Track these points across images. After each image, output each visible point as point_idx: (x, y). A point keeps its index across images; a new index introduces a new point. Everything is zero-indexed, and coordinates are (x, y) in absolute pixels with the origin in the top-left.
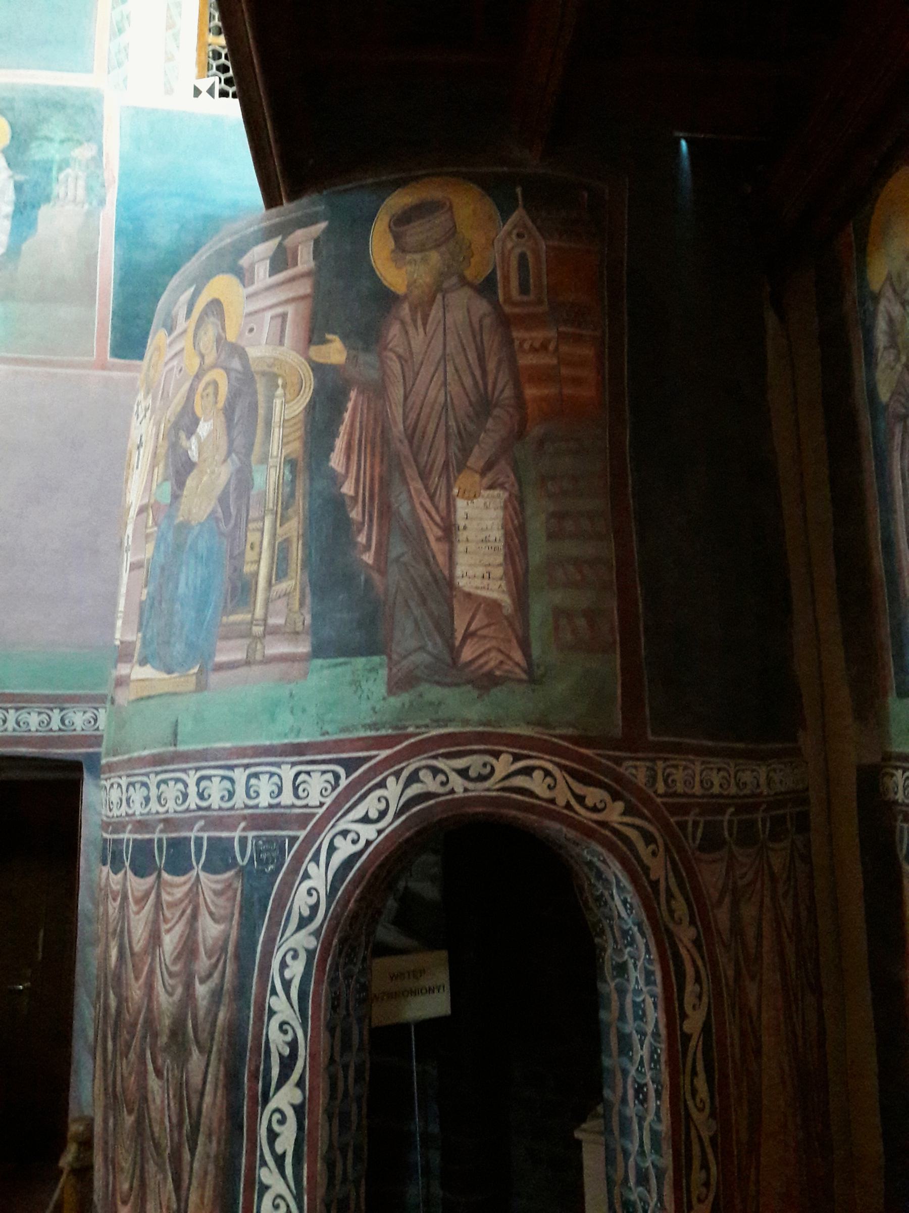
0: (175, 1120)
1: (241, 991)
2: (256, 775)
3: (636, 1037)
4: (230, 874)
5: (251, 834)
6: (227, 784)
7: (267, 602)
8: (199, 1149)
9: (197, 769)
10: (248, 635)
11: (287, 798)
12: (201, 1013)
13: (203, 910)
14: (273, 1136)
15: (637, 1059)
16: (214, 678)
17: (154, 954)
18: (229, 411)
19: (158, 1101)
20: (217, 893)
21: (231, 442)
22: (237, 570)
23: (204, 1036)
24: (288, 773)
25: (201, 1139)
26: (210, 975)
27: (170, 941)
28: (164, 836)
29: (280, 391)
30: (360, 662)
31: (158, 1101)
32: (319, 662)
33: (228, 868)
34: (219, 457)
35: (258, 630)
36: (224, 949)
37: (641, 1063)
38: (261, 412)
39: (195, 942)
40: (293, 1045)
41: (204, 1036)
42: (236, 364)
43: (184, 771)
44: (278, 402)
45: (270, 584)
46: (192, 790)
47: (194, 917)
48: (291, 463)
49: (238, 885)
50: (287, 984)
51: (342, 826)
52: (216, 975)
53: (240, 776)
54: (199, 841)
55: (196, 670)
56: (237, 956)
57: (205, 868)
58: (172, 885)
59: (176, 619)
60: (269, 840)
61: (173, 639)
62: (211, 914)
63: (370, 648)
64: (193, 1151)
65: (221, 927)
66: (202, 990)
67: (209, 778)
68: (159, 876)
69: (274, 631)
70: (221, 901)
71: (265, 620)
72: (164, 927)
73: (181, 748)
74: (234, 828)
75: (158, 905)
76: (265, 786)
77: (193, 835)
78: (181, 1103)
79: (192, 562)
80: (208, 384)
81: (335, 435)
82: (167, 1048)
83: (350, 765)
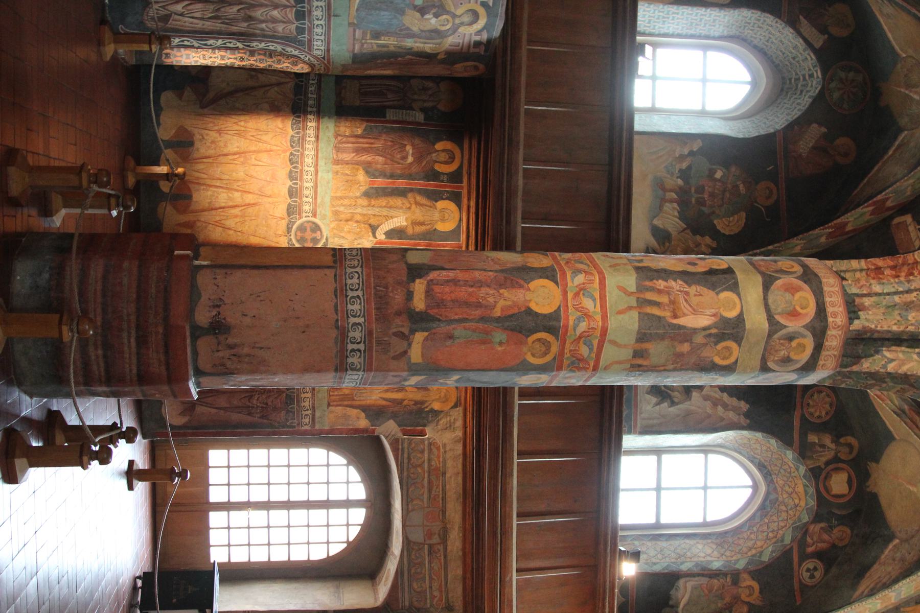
0: (227, 17)
1: (265, 36)
2: (322, 41)
3: (255, 58)
4: (295, 33)
5: (306, 39)
6: (320, 34)
7: (372, 43)
8: (223, 25)
9: (325, 24)
10: (363, 39)
11: (315, 47)
12: (258, 26)
13: (285, 25)
14: (230, 43)
15: (250, 58)
16: (352, 29)
17: (271, 6)
18: (436, 31)
19: (231, 11)
20: (290, 30)
21: (424, 31)
22: (383, 35)
23: (251, 26)
24: (322, 48)
25: (225, 26)
26: (267, 27)
27: (275, 13)
28: (306, 9)
29: (434, 46)
30: (350, 61)
31: (231, 11)
32: (352, 55)
33: (297, 33)
34: (422, 28)
35: (364, 41)
36: (275, 32)
37: (249, 60)
38: (430, 41)
39: (276, 23)
40: (253, 47)
41: (251, 26)
42: (450, 32)
43: (325, 20)
44: (431, 45)
45: (376, 43)
46: (319, 22)
47: (284, 22)
48: (411, 49)
49: (293, 36)
50: (268, 46)
51: (308, 56)
52: (267, 29)
53: (322, 38)
54: (304, 24)
55: (355, 22)
56: (274, 35)
57: (297, 26)
58: (292, 13)
59: (373, 12)
60: (305, 44)
61: (367, 10)
62: (284, 28)
63: (353, 62)
64: (222, 23)
65: (281, 31)
66: (263, 25)
67: (322, 28)
68: (295, 7)
69: (362, 45)
70: (288, 31)
71: (366, 43)
72: (279, 10)
73: (332, 18)
74: (308, 35)
75: (286, 7)
76: (319, 43)
77: (306, 22)
78: (232, 19)
79: (390, 17)
80: (448, 21)
81: (416, 57)
82: (246, 14)
83: (324, 58)
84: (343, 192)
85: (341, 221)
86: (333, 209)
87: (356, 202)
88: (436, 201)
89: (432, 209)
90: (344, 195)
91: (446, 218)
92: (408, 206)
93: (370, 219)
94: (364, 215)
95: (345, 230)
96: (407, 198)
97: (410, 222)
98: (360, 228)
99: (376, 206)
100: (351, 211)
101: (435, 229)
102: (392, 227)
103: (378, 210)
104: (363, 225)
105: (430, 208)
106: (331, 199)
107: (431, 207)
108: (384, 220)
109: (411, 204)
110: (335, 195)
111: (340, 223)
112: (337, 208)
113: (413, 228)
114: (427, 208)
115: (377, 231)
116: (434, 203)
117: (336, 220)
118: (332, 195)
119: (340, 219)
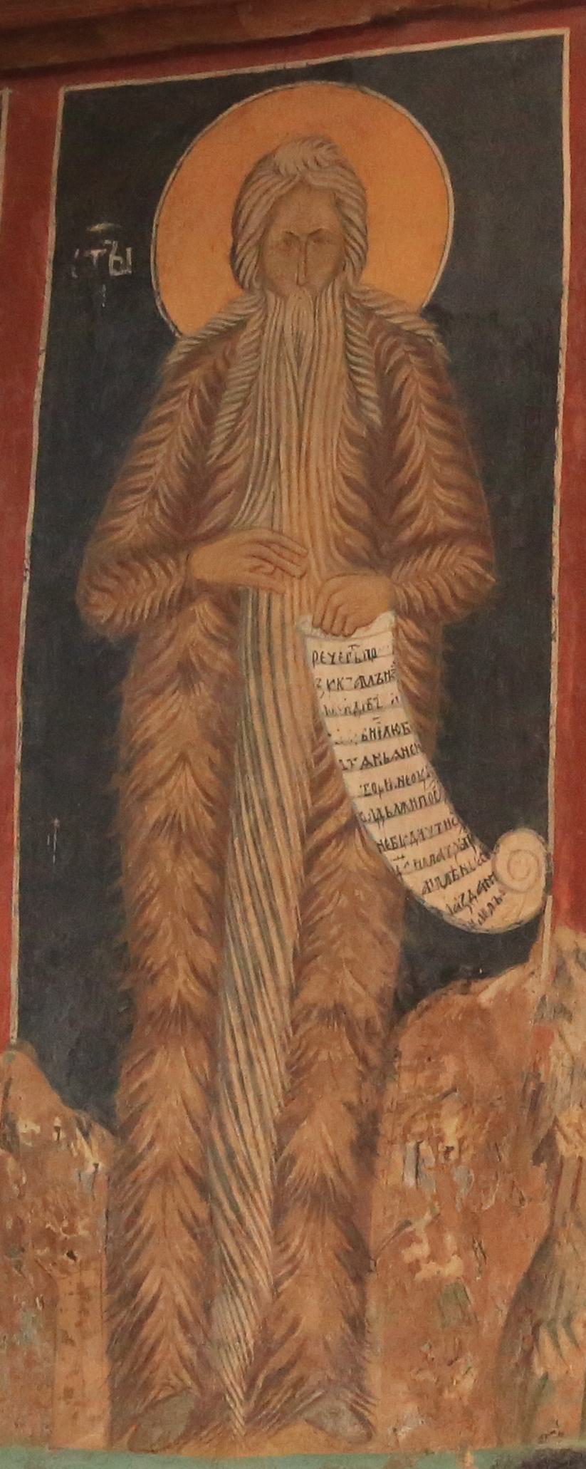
84: (68, 1318)
85: (357, 1324)
86: (240, 1412)
87: (164, 1172)
88: (163, 335)
89: (239, 374)
90: (98, 1303)
91: (324, 218)
92: (204, 610)
93: (337, 1012)
94: (297, 1069)
95: (453, 1268)
96: (130, 639)
97: (371, 587)
98: (433, 1111)
99: (205, 953)
100: (259, 1223)
101: (433, 311)
102: (419, 763)
103: (248, 931)
104: (404, 1085)
105: (232, 394)
106: (139, 1446)
107: (216, 387)
108: (353, 857)
109: (186, 597)
110: (98, 1407)
111: (378, 1331)
112: (231, 1369)
113: (423, 543)
114: (224, 420)
115: (464, 918)
116: (174, 358)
117: (356, 1378)
118: (96, 1435)
119: (337, 1330)
